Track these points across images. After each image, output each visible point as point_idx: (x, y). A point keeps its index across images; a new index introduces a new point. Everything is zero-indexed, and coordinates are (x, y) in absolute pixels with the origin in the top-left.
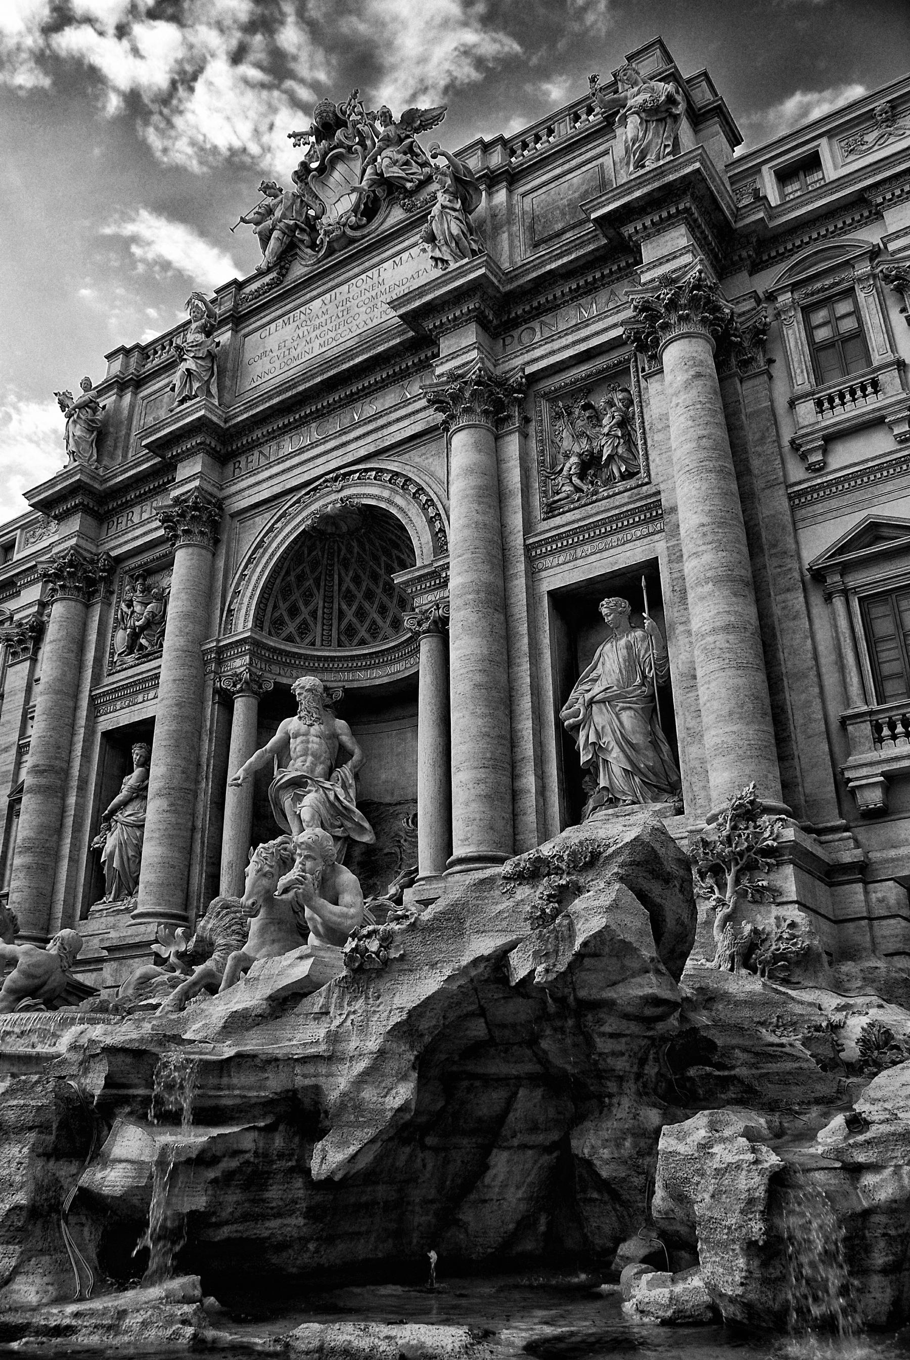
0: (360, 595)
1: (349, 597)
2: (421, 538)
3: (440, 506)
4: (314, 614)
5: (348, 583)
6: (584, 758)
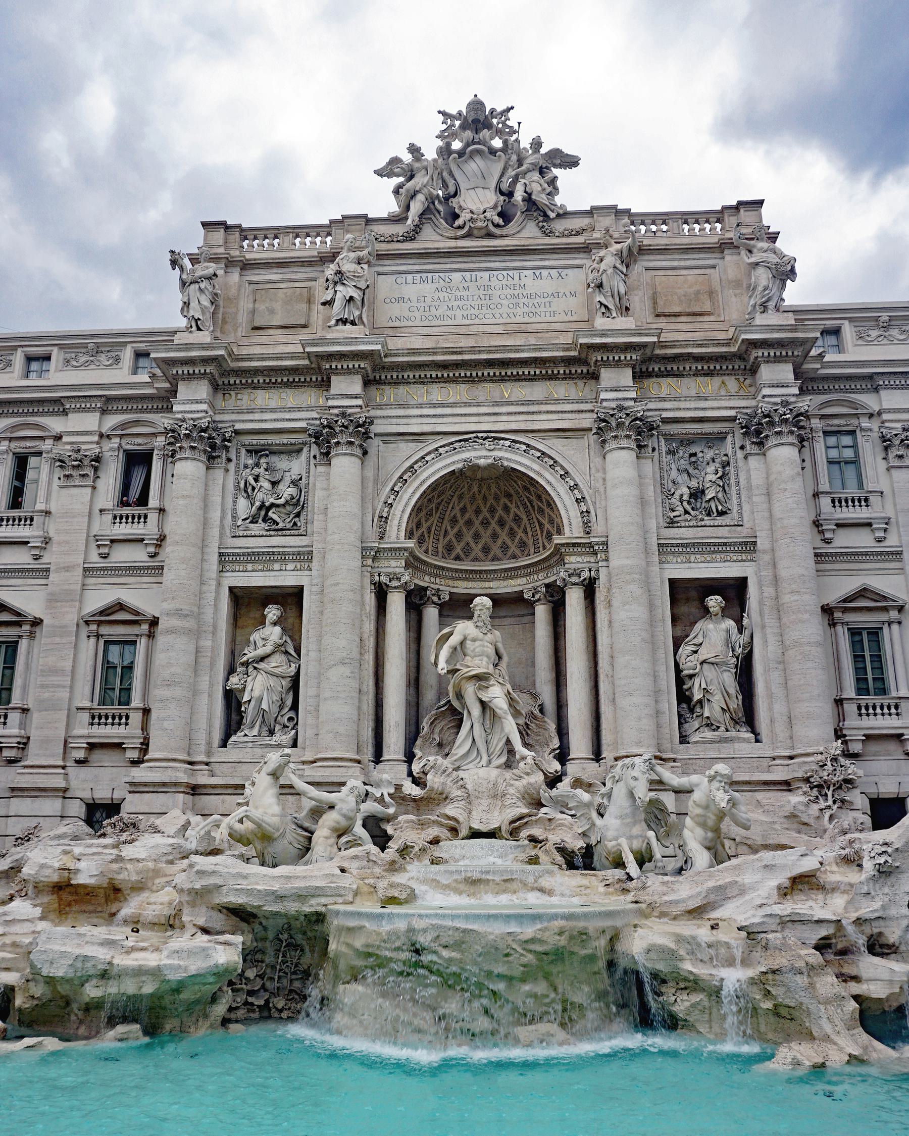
0: (461, 522)
1: (454, 521)
3: (586, 493)
5: (457, 511)
6: (697, 696)
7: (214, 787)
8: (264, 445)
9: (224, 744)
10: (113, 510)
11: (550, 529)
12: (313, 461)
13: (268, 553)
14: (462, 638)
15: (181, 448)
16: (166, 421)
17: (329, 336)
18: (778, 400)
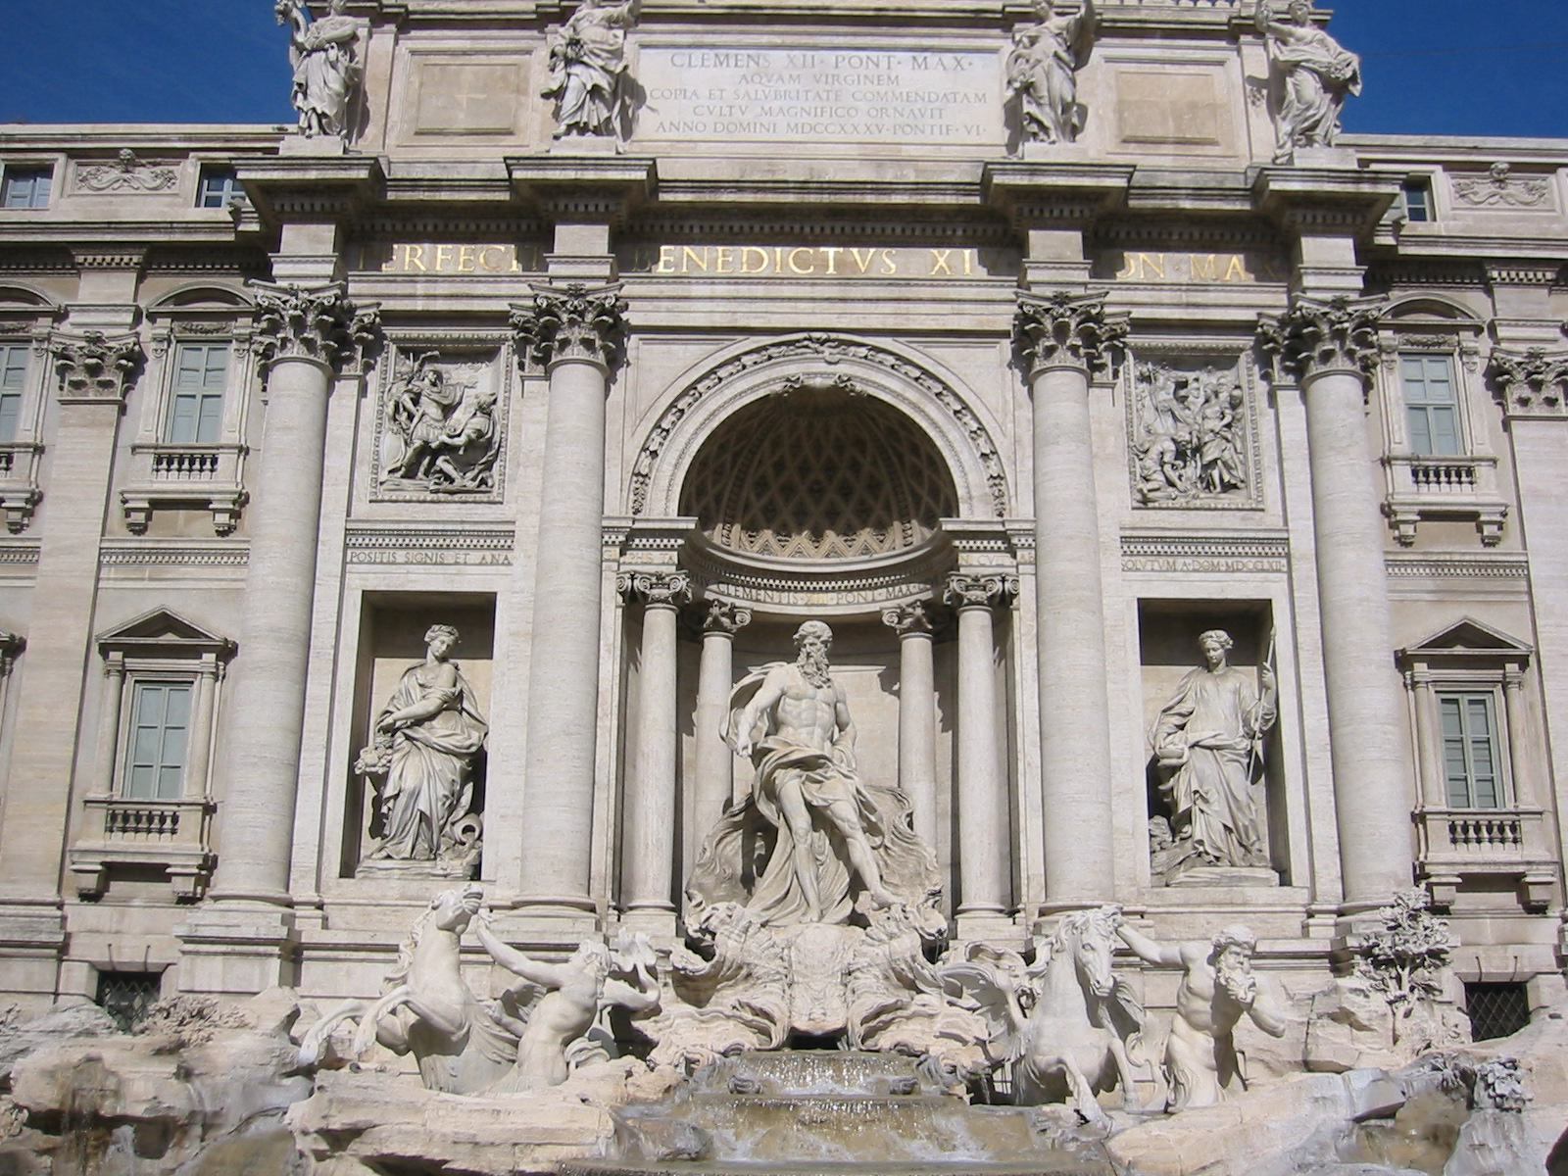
1: (762, 485)
4: (718, 499)
6: (1182, 807)
7: (335, 947)
8: (427, 340)
9: (349, 868)
10: (156, 448)
12: (516, 373)
13: (435, 533)
14: (778, 693)
15: (285, 341)
16: (261, 292)
17: (552, 154)
18: (1328, 296)
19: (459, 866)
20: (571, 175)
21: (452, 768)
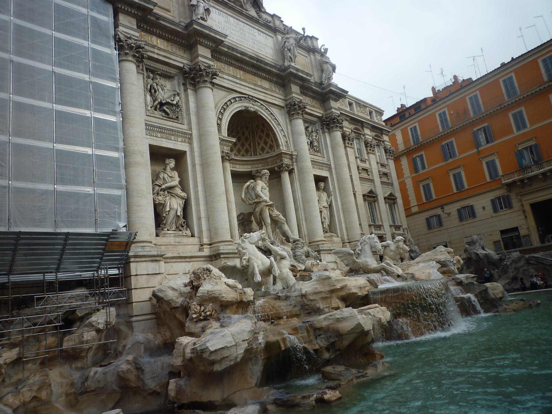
2: (281, 140)
8: (156, 68)
9: (157, 235)
11: (264, 146)
13: (170, 130)
19: (189, 233)
20: (207, 32)
21: (181, 202)
